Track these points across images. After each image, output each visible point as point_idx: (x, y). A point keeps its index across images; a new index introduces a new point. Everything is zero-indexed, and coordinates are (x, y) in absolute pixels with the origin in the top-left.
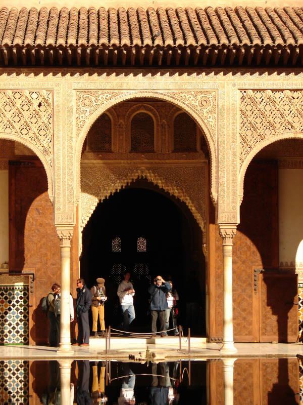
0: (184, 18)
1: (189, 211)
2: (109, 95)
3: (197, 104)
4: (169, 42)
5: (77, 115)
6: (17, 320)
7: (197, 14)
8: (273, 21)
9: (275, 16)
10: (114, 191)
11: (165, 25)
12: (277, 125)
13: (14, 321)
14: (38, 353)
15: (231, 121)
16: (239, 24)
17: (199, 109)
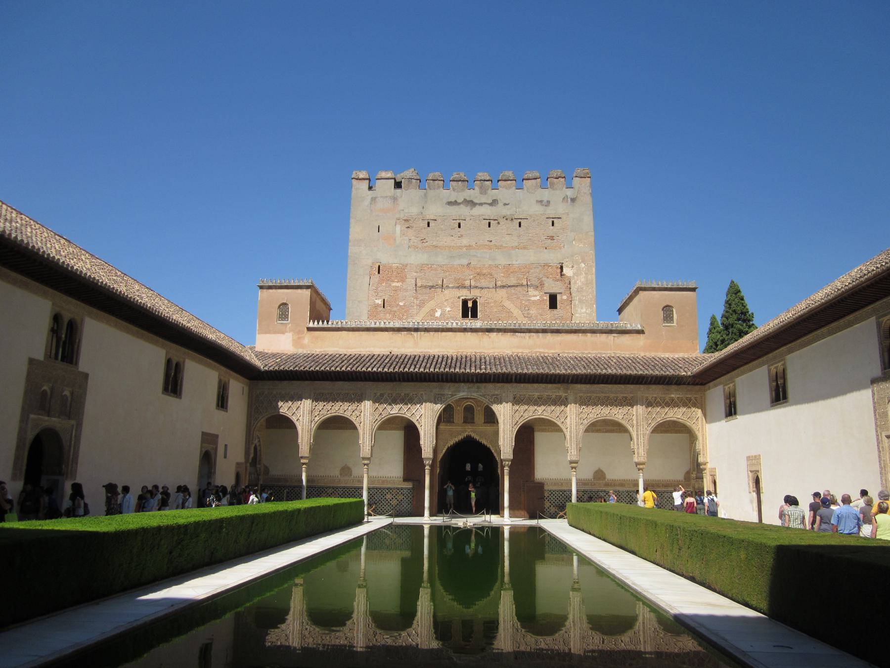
0: (487, 358)
1: (491, 452)
3: (492, 400)
4: (478, 371)
10: (455, 442)
11: (478, 363)
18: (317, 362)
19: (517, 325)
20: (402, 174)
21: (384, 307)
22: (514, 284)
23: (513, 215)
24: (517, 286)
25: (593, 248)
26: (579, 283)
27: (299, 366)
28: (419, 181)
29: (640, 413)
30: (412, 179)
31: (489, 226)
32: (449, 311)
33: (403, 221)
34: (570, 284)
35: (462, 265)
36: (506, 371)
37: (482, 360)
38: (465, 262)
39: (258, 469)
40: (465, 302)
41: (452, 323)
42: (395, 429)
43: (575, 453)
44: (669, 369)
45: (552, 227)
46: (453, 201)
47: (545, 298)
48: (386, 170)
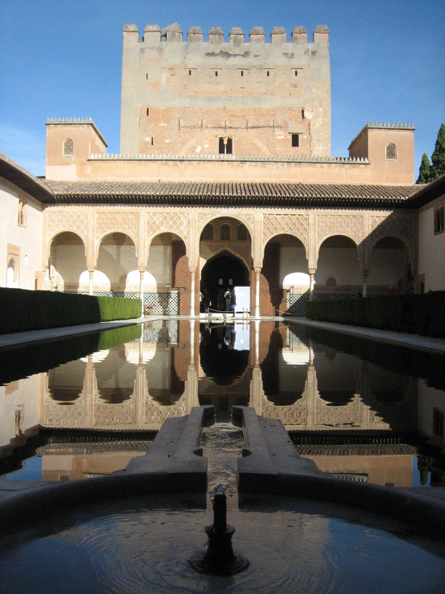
0: (242, 186)
1: (244, 263)
2: (211, 216)
4: (235, 194)
5: (198, 223)
6: (175, 306)
7: (248, 185)
8: (277, 188)
9: (278, 186)
10: (214, 255)
11: (234, 189)
12: (278, 229)
13: (173, 306)
14: (182, 317)
15: (260, 226)
16: (264, 189)
17: (247, 221)
18: (98, 188)
19: (266, 158)
20: (167, 28)
21: (152, 144)
22: (263, 125)
23: (263, 65)
24: (265, 127)
25: (330, 96)
26: (317, 125)
27: (84, 190)
28: (181, 34)
29: (366, 232)
30: (175, 32)
31: (242, 75)
32: (207, 148)
33: (169, 70)
34: (309, 126)
35: (218, 108)
36: (258, 195)
37: (236, 186)
38: (220, 105)
39: (52, 278)
40: (221, 140)
41: (212, 157)
42: (165, 244)
43: (313, 262)
44: (391, 194)
45: (295, 77)
46: (211, 52)
47: (289, 137)
48: (152, 24)
